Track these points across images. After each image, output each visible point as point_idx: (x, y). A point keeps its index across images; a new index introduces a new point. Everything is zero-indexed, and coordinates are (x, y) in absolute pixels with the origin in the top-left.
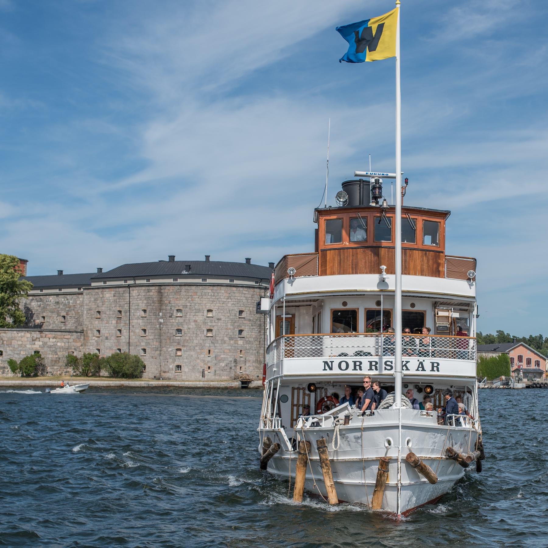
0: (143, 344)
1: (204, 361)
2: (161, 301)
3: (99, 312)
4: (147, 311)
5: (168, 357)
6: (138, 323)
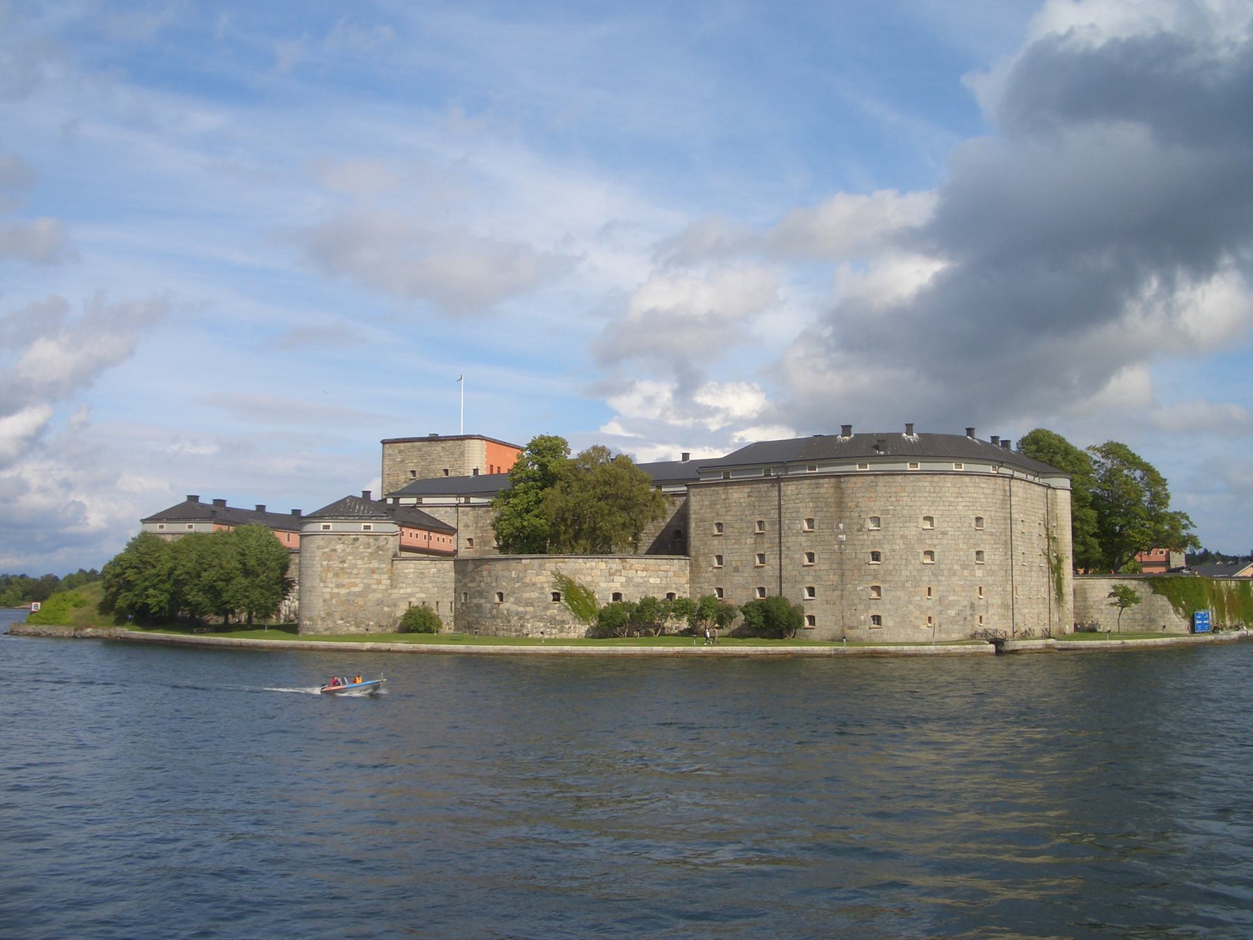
0: (810, 578)
1: (921, 607)
2: (840, 504)
3: (719, 525)
4: (816, 524)
5: (857, 601)
6: (798, 544)
